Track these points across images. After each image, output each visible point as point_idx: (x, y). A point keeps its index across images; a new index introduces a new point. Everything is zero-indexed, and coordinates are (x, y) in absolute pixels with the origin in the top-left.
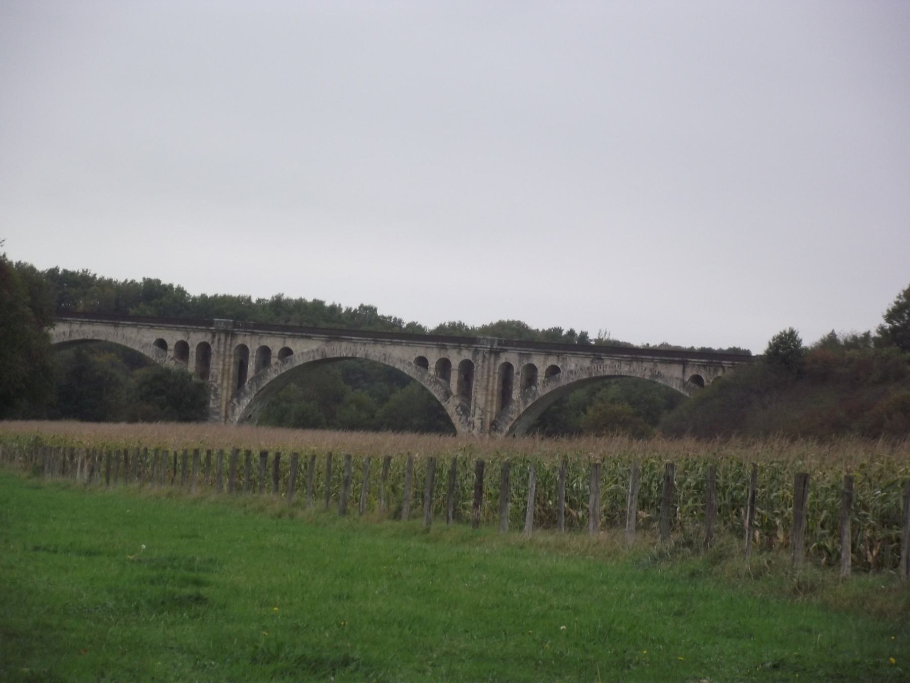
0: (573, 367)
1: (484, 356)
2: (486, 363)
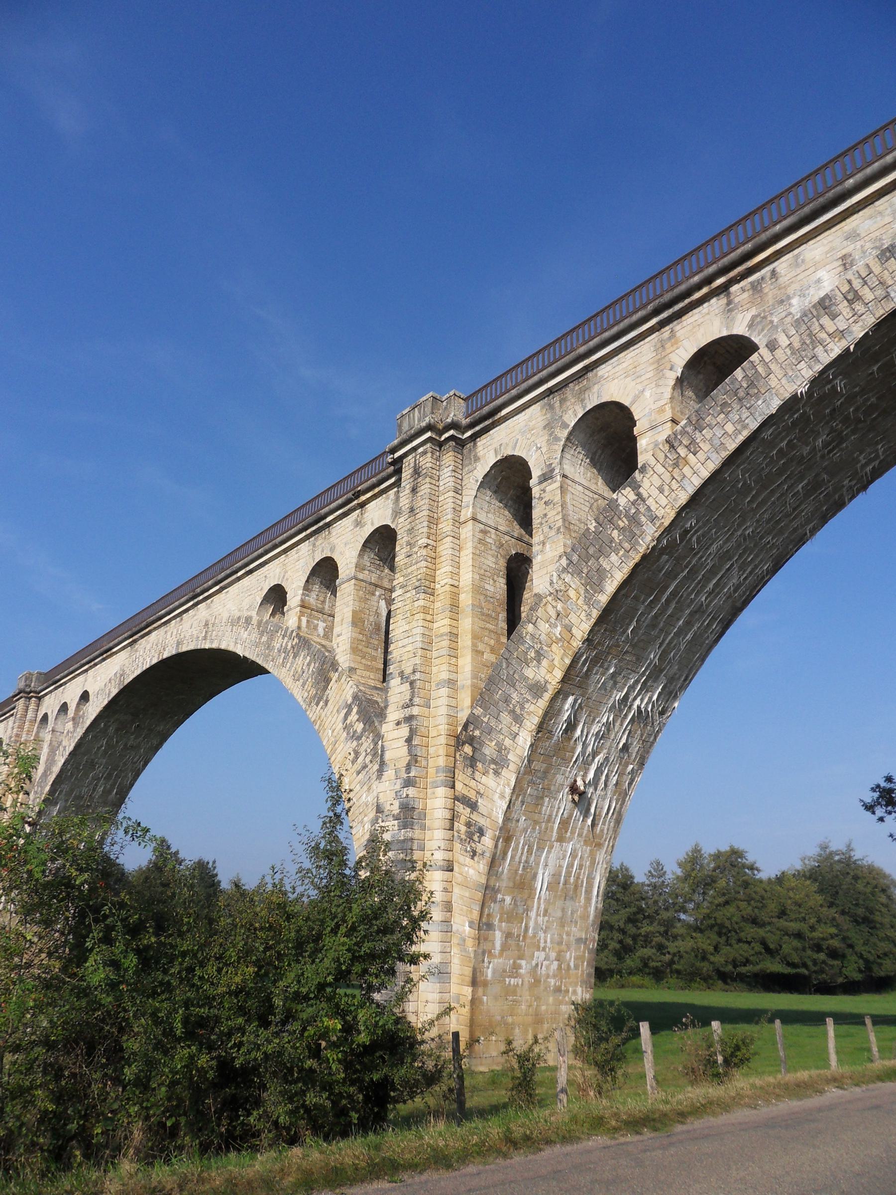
0: (828, 280)
1: (417, 472)
2: (425, 488)
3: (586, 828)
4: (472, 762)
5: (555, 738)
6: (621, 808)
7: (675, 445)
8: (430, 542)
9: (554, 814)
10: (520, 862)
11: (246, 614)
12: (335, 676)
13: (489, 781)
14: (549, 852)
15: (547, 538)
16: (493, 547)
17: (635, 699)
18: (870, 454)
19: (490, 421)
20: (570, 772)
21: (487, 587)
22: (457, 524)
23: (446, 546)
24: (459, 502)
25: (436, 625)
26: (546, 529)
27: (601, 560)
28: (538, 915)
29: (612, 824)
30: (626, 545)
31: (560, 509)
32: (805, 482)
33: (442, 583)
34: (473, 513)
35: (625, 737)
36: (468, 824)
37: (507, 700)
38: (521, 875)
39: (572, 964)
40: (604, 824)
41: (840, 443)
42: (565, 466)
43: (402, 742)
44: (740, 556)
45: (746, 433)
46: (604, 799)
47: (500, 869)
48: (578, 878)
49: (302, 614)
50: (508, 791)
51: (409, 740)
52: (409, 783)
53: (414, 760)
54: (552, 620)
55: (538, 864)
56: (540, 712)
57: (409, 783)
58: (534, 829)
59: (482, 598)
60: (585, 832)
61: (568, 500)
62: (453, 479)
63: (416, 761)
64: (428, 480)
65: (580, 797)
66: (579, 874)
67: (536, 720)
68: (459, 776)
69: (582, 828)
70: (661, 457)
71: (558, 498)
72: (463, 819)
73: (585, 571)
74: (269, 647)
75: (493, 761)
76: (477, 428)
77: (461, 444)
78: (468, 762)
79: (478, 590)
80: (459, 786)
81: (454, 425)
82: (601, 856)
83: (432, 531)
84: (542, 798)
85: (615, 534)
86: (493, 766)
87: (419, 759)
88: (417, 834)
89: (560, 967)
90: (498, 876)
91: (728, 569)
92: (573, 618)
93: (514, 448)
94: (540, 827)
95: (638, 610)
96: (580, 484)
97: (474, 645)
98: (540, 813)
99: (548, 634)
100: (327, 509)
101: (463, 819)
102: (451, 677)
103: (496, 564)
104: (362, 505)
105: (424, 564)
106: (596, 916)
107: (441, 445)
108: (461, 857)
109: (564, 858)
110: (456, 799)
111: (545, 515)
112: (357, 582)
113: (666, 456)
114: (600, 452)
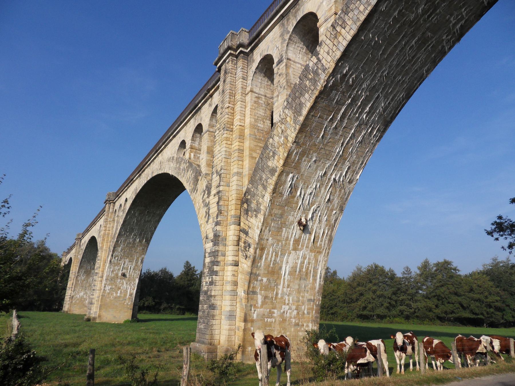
3: (311, 244)
4: (247, 211)
5: (285, 196)
6: (331, 233)
7: (335, 26)
8: (230, 105)
9: (290, 236)
10: (271, 261)
11: (173, 155)
12: (200, 178)
13: (253, 220)
14: (289, 256)
15: (279, 93)
16: (263, 105)
17: (331, 175)
18: (457, 16)
19: (258, 39)
20: (297, 215)
21: (259, 125)
22: (244, 95)
23: (238, 106)
24: (245, 84)
25: (233, 146)
26: (279, 88)
27: (301, 99)
28: (283, 287)
29: (327, 242)
30: (312, 88)
31: (285, 77)
32: (417, 38)
33: (236, 125)
34: (251, 88)
35: (329, 195)
36: (245, 243)
37: (261, 179)
38: (272, 268)
39: (306, 312)
40: (322, 241)
41: (435, 10)
42: (289, 54)
43: (215, 205)
44: (384, 89)
45: (370, 8)
46: (320, 229)
47: (259, 264)
48: (308, 269)
49: (191, 152)
50: (260, 225)
51: (218, 203)
52: (217, 224)
53: (220, 212)
54: (280, 135)
55: (282, 262)
56: (274, 183)
57: (217, 224)
58: (278, 244)
59: (256, 130)
60: (310, 246)
61: (291, 72)
62: (242, 73)
63: (221, 213)
64: (230, 75)
65: (304, 227)
66: (308, 267)
67: (272, 187)
68: (242, 219)
69: (308, 243)
70: (329, 34)
71: (284, 71)
72: (243, 240)
73: (294, 106)
74: (179, 169)
75: (255, 211)
76: (253, 45)
77: (247, 55)
78: (245, 212)
79: (253, 126)
80: (242, 224)
81: (241, 45)
82: (321, 258)
83: (231, 100)
84: (281, 228)
85: (307, 83)
86: (255, 213)
87: (223, 212)
88: (221, 248)
89: (298, 313)
90: (258, 268)
91: (377, 98)
92: (289, 132)
93: (267, 51)
94: (282, 243)
95: (324, 124)
96: (299, 63)
97: (250, 154)
98: (281, 235)
99: (278, 143)
100: (198, 101)
101: (243, 240)
102: (239, 171)
103: (265, 113)
104: (211, 96)
105: (227, 116)
106: (319, 288)
107: (237, 57)
108: (242, 260)
109: (298, 259)
110: (240, 231)
111: (279, 81)
112: (209, 133)
113: (331, 34)
114: (310, 46)
